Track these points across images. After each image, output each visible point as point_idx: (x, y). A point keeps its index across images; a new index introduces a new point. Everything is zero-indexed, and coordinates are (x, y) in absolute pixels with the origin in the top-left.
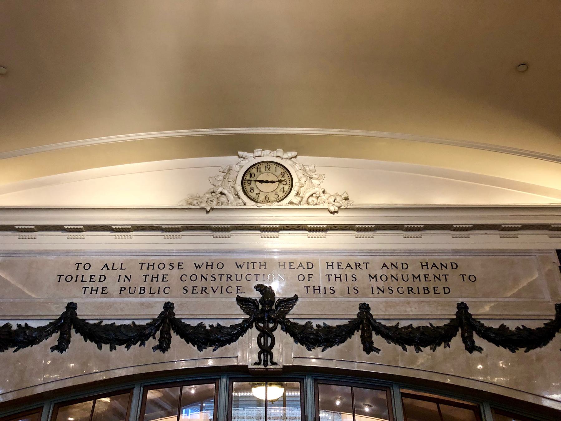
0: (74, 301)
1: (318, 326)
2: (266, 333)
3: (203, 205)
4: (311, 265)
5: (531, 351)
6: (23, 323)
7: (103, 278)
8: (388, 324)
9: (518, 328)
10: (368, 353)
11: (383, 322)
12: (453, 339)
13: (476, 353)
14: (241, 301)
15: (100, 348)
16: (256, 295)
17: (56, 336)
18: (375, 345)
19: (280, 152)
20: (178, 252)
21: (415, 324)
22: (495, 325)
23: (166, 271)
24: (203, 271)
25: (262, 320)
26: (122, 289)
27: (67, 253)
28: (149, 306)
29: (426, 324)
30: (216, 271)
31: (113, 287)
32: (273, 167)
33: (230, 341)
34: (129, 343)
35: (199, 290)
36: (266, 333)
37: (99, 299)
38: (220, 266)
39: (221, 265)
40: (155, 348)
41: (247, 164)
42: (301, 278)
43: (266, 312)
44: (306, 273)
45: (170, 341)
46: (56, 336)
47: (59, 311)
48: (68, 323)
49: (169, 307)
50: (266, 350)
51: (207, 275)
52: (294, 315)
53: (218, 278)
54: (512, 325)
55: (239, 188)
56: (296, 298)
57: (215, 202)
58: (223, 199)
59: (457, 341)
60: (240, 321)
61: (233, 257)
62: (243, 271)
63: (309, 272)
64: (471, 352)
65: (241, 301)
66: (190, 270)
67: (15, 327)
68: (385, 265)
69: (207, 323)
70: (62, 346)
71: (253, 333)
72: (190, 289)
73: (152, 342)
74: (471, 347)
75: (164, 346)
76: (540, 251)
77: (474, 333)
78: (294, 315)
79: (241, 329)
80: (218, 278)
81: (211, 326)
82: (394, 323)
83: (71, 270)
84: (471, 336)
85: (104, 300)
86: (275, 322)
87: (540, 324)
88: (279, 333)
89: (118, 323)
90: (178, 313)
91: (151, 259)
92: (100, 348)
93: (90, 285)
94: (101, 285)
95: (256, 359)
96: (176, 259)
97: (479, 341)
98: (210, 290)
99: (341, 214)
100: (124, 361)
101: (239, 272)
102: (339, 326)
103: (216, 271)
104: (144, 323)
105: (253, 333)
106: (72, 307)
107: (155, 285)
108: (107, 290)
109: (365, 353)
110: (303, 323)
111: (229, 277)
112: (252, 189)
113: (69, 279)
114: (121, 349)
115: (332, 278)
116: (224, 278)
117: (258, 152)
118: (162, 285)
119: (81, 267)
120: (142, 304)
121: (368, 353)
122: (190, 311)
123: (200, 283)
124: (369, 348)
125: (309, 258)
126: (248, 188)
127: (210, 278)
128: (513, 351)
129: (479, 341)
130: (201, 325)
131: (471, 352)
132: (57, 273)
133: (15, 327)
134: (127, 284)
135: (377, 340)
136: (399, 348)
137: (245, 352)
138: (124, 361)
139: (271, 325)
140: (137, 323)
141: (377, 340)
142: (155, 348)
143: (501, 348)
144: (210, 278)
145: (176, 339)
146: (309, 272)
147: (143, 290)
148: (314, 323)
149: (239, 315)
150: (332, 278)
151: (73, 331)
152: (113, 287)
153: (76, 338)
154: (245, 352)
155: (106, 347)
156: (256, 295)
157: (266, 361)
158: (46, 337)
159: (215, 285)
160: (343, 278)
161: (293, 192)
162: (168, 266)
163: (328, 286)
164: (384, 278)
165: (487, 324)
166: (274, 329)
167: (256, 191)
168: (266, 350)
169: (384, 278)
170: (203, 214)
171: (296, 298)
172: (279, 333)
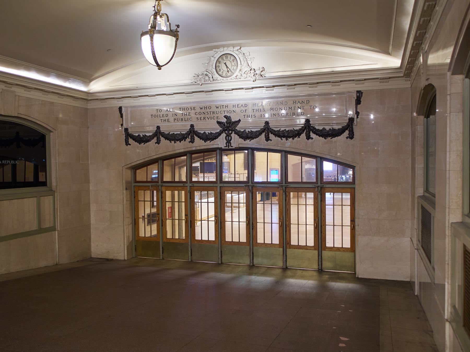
0: (159, 125)
1: (248, 131)
2: (228, 135)
3: (198, 82)
4: (246, 105)
5: (333, 139)
6: (144, 134)
7: (167, 115)
8: (276, 129)
9: (330, 129)
10: (267, 141)
11: (274, 129)
12: (302, 135)
13: (310, 140)
14: (219, 123)
15: (171, 142)
16: (224, 120)
17: (155, 138)
18: (270, 138)
19: (231, 48)
20: (193, 102)
21: (287, 129)
22: (321, 128)
23: (189, 111)
24: (203, 110)
25: (226, 130)
26: (175, 119)
27: (152, 105)
28: (185, 126)
29: (291, 129)
30: (208, 110)
31: (172, 119)
32: (229, 56)
33: (215, 139)
34: (180, 140)
35: (202, 118)
36: (228, 135)
37: (167, 124)
38: (210, 108)
39: (210, 107)
40: (189, 142)
41: (217, 56)
42: (242, 111)
43: (229, 126)
44: (244, 109)
45: (194, 139)
46: (155, 138)
47: (154, 129)
48: (158, 134)
49: (192, 126)
50: (229, 142)
51: (205, 111)
52: (239, 127)
53: (209, 113)
54: (327, 128)
55: (214, 70)
56: (240, 120)
57: (203, 81)
58: (207, 78)
59: (303, 136)
60: (218, 131)
61: (215, 103)
62: (219, 110)
63: (245, 108)
64: (308, 140)
65: (219, 123)
66: (198, 110)
67: (142, 136)
68: (278, 103)
69: (207, 132)
70: (158, 142)
71: (224, 135)
72: (199, 118)
73: (188, 140)
74: (308, 137)
75: (192, 141)
76: (349, 92)
77: (311, 132)
78: (239, 127)
79: (219, 134)
80: (209, 113)
81: (208, 133)
82: (278, 129)
83: (155, 113)
84: (310, 133)
85: (169, 124)
86: (232, 131)
87: (340, 127)
88: (233, 135)
89: (175, 133)
90: (196, 128)
91: (184, 106)
92: (171, 142)
93: (163, 118)
94: (167, 118)
95: (225, 145)
96: (193, 105)
97: (312, 135)
98: (207, 119)
99: (257, 82)
100: (180, 146)
101: (217, 110)
102: (256, 131)
103: (208, 110)
104: (184, 133)
105: (224, 135)
106: (158, 127)
107: (186, 117)
108: (169, 120)
109: (266, 141)
110: (242, 130)
111: (213, 113)
112: (220, 70)
113: (156, 116)
114: (178, 142)
115: (255, 111)
116: (212, 113)
117: (222, 49)
118: (189, 117)
119: (158, 111)
120: (182, 125)
121: (267, 141)
122: (201, 127)
123: (203, 116)
124: (267, 139)
125: (245, 102)
126: (218, 70)
127: (206, 113)
128: (325, 139)
129: (312, 135)
130: (204, 133)
131: (308, 140)
132: (150, 114)
133: (142, 136)
134: (176, 117)
135: (271, 136)
136: (280, 139)
137: (221, 142)
138: (180, 146)
139: (230, 132)
140: (182, 133)
141: (271, 136)
142: (189, 142)
143: (321, 138)
144: (206, 113)
145: (196, 138)
146: (245, 108)
147: (182, 119)
148: (247, 130)
149: (218, 129)
150: (255, 111)
151: (161, 136)
152: (172, 119)
153: (162, 139)
154: (221, 142)
155: (173, 142)
156: (224, 120)
157: (229, 146)
158: (153, 139)
159: (208, 116)
160: (259, 110)
161: (238, 70)
162: (190, 109)
163: (253, 115)
164: (276, 109)
165: (317, 128)
166: (232, 133)
167: (222, 71)
168: (229, 142)
169: (276, 109)
170: (200, 86)
171: (240, 120)
172: (233, 135)
